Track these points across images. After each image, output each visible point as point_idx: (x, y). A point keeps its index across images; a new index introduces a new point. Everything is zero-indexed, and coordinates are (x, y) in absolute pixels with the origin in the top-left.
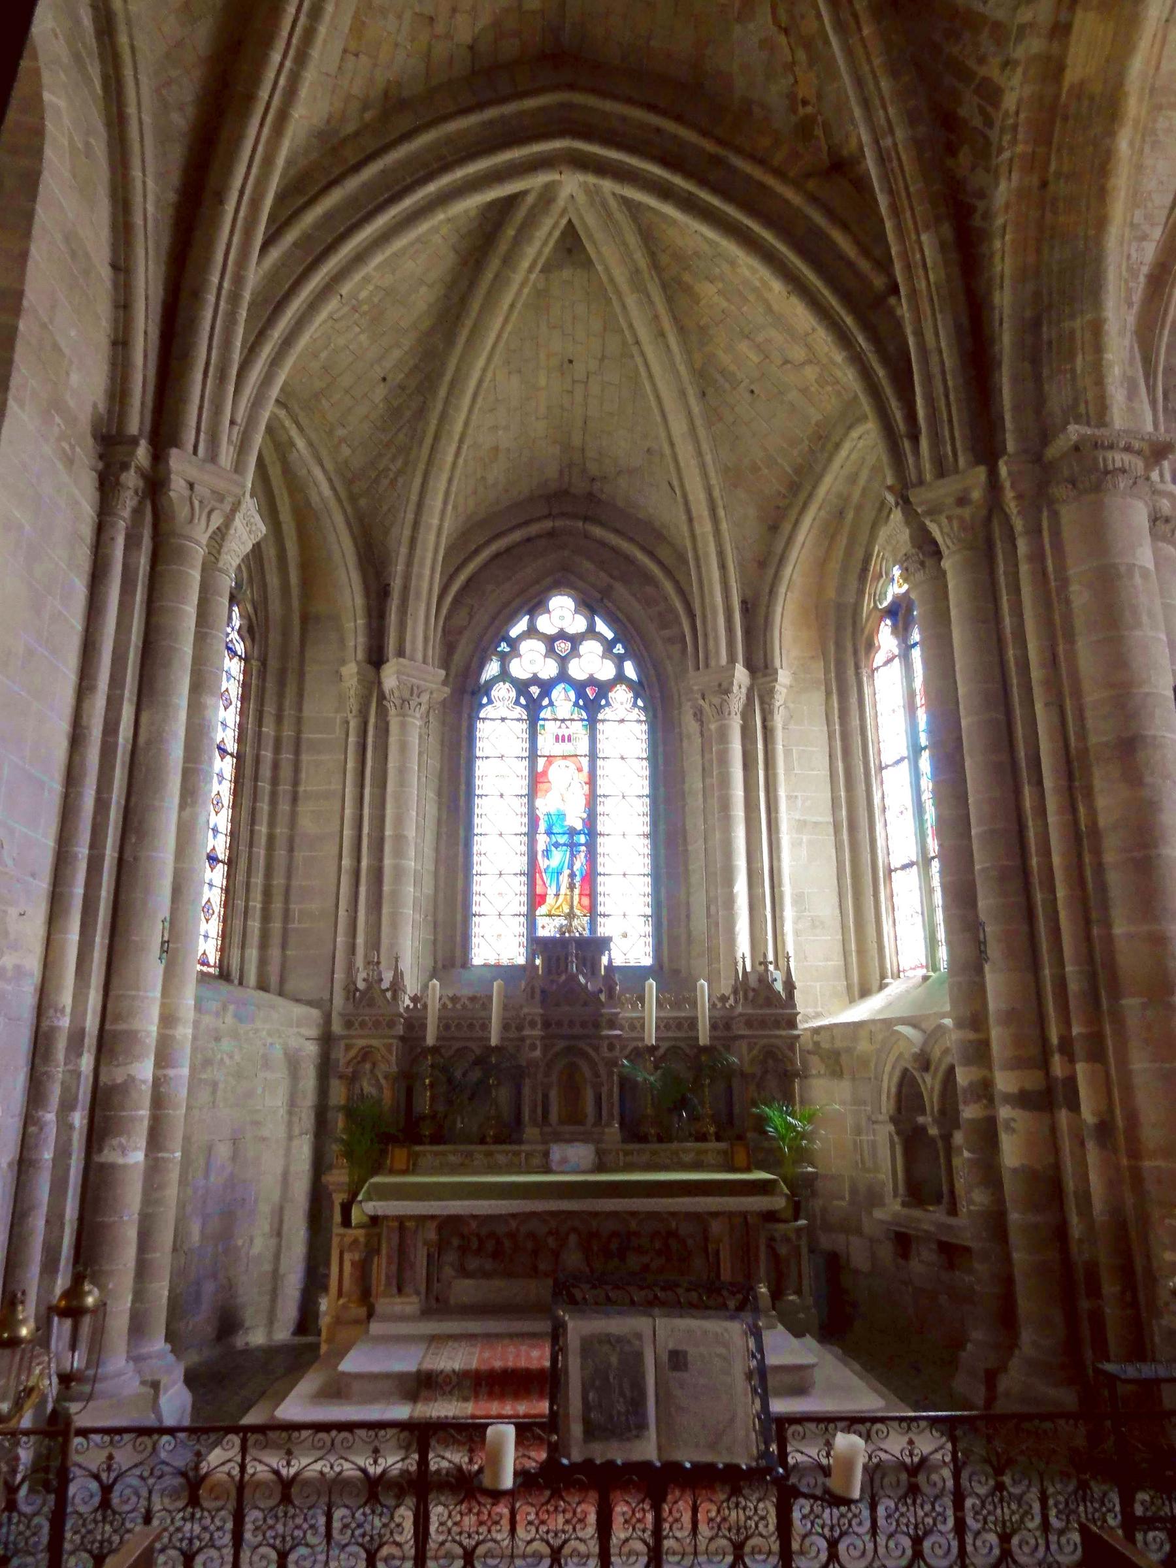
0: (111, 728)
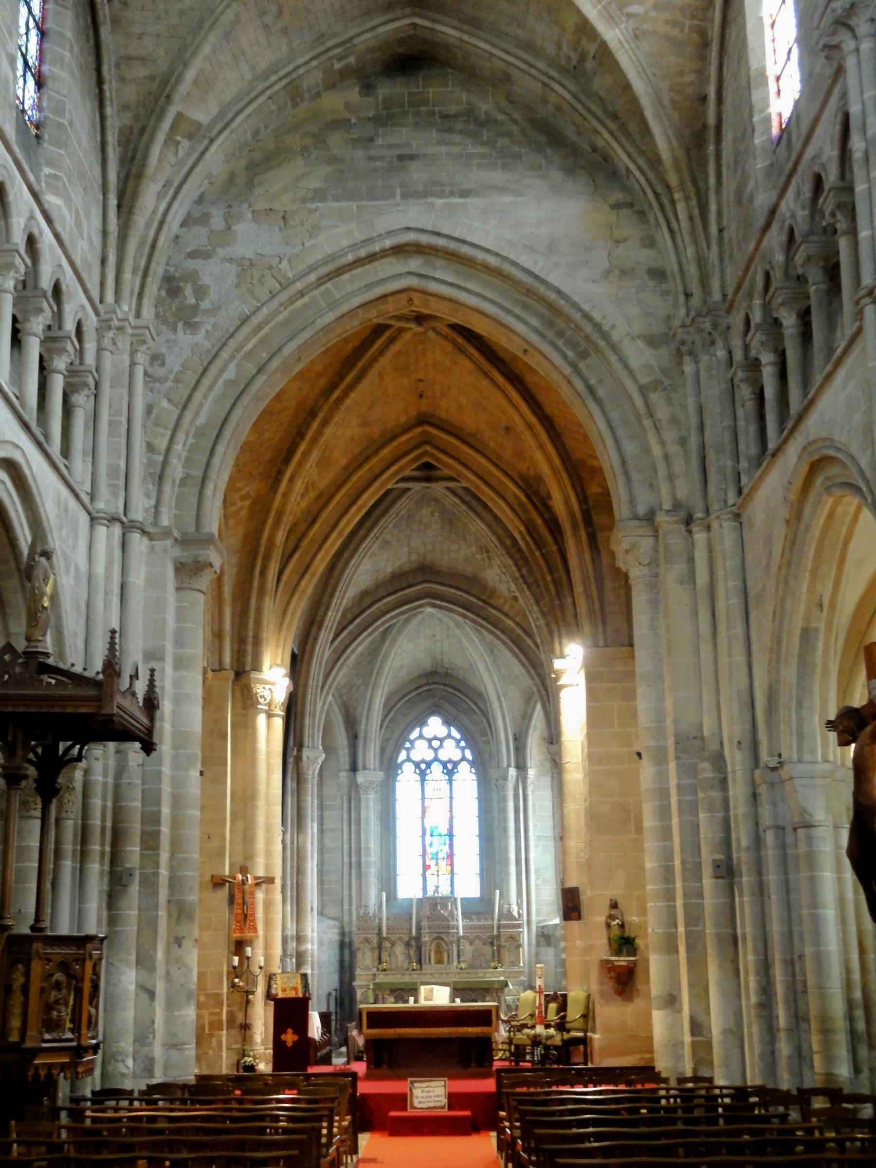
0: (292, 843)
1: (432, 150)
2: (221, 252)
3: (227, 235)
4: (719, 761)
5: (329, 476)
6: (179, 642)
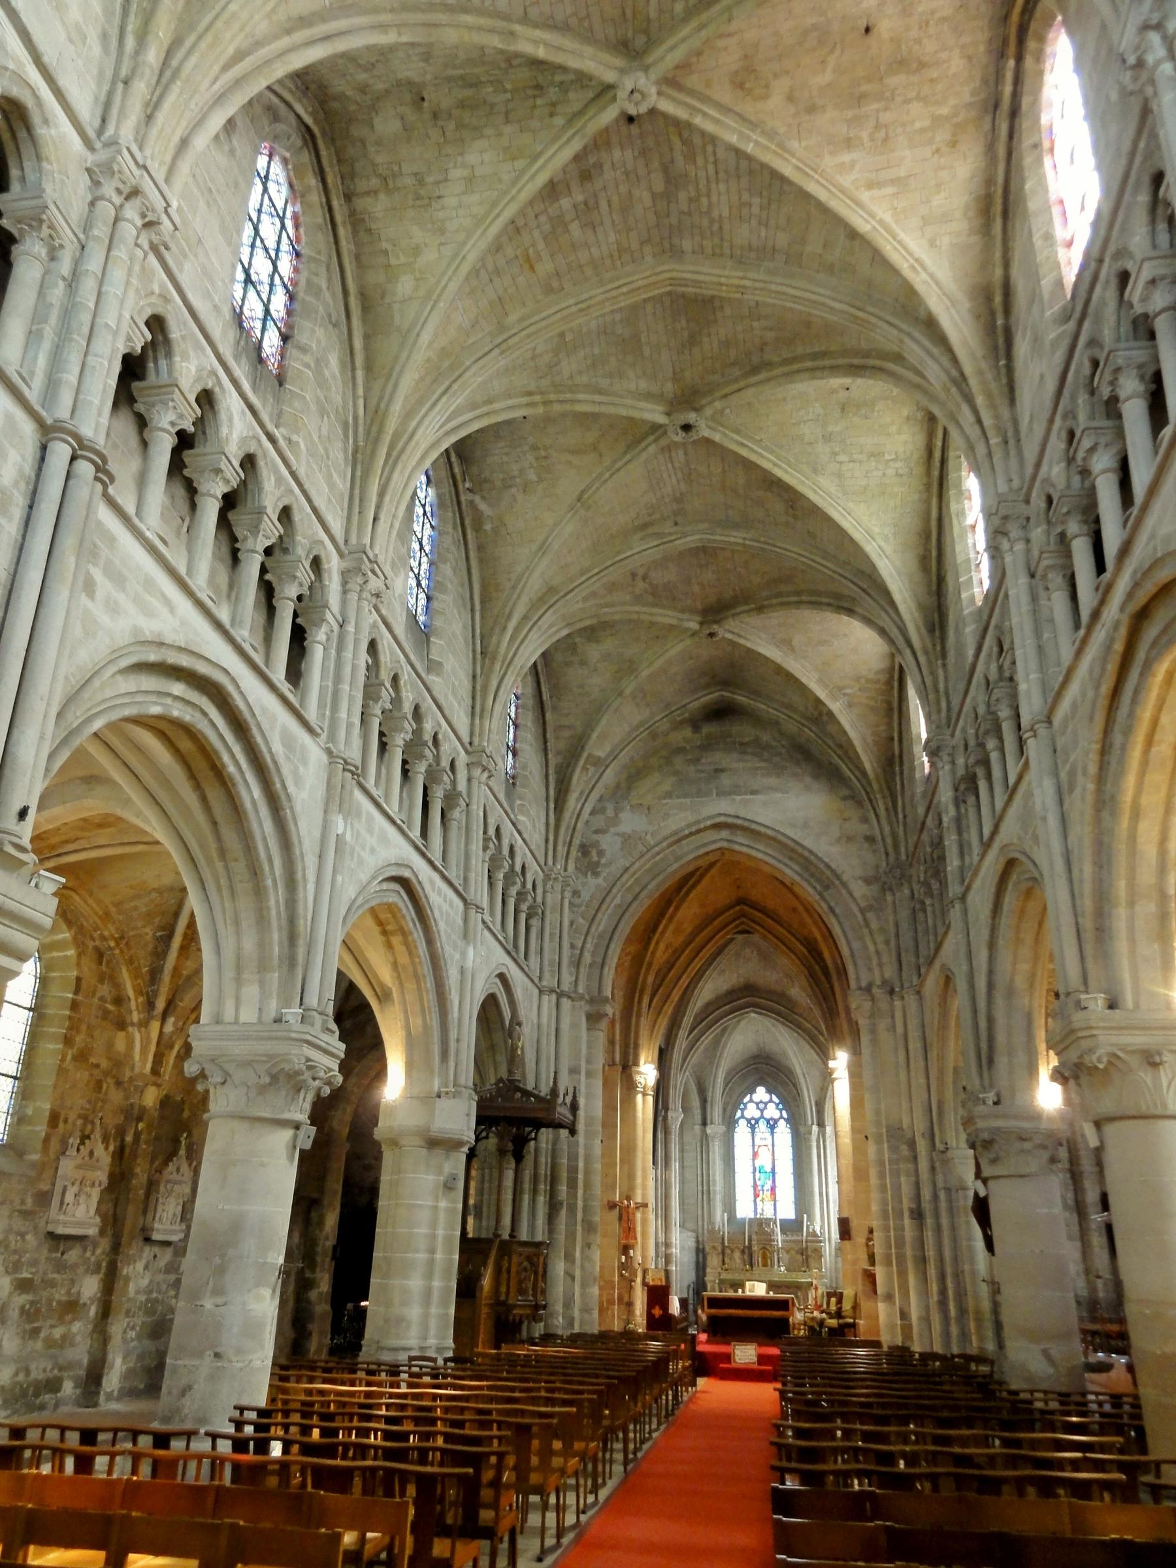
1: (734, 765)
2: (612, 830)
3: (615, 821)
4: (912, 1144)
5: (681, 939)
6: (588, 1062)
